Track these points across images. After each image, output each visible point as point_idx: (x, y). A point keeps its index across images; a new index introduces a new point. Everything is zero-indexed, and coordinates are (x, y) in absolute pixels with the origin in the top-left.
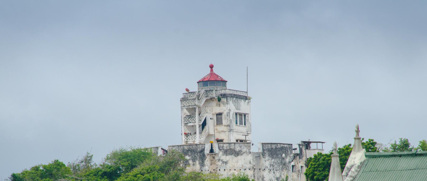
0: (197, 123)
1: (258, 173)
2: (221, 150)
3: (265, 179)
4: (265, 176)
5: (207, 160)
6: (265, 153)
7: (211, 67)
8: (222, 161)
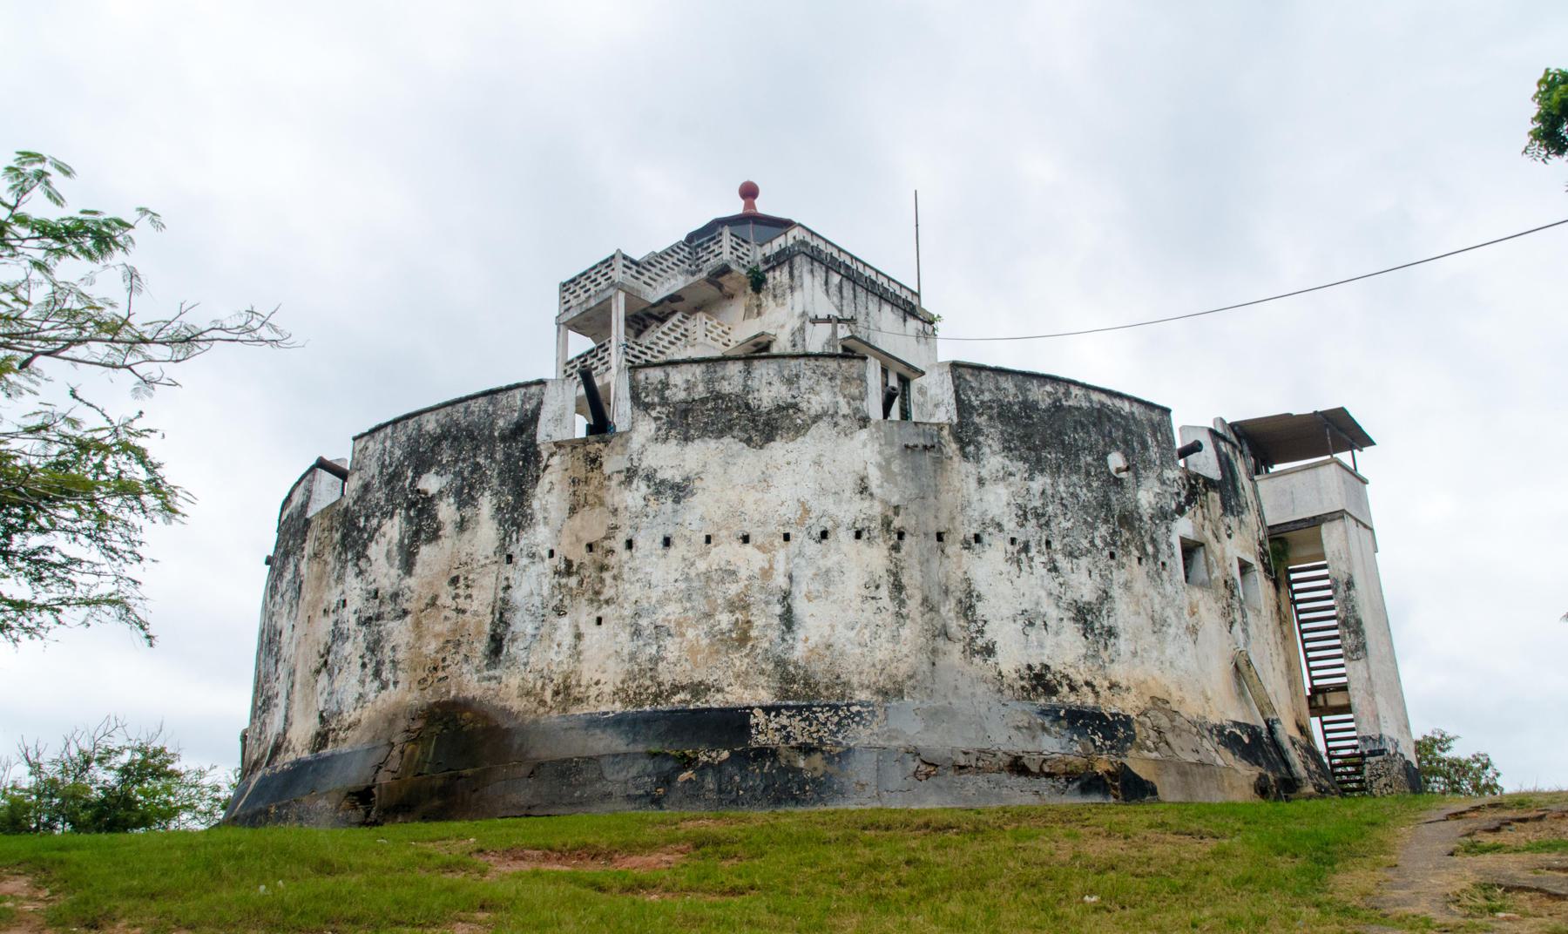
0: (614, 370)
2: (647, 407)
3: (981, 609)
4: (980, 587)
5: (546, 480)
6: (978, 431)
7: (749, 192)
8: (648, 478)
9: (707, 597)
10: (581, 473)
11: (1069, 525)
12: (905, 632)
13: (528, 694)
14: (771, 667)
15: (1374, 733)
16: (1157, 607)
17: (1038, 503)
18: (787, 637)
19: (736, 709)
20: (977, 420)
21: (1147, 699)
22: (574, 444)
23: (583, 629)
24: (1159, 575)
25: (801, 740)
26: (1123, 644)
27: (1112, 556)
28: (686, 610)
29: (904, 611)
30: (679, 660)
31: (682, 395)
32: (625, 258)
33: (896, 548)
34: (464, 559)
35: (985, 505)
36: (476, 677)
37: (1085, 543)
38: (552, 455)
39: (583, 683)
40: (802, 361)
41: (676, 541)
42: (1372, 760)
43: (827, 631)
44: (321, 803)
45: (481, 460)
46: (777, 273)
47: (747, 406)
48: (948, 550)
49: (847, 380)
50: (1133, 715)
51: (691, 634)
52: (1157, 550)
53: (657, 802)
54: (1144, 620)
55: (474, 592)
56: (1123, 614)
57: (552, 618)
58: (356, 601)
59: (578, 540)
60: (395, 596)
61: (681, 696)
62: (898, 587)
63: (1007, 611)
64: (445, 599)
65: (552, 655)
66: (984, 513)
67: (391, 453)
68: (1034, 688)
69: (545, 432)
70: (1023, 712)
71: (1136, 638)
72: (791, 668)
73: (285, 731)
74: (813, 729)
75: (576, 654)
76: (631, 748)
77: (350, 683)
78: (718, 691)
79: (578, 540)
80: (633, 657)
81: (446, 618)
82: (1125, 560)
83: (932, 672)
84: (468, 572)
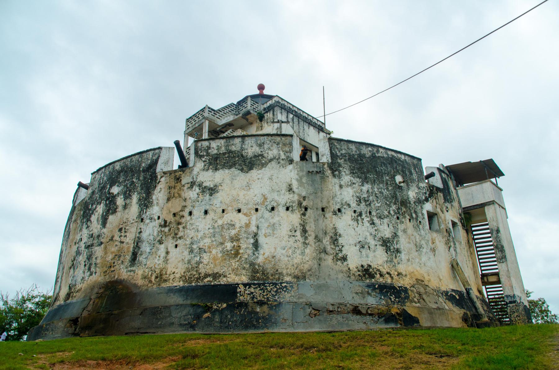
1: (316, 221)
2: (201, 157)
3: (341, 241)
6: (340, 165)
7: (261, 87)
8: (200, 186)
9: (222, 235)
10: (173, 184)
11: (379, 205)
12: (307, 251)
13: (145, 278)
14: (247, 266)
15: (512, 294)
16: (418, 240)
17: (366, 196)
18: (256, 253)
19: (231, 285)
20: (339, 161)
21: (414, 280)
22: (171, 172)
23: (169, 250)
24: (418, 226)
25: (259, 299)
26: (403, 256)
27: (398, 218)
28: (212, 241)
29: (307, 242)
30: (208, 263)
31: (215, 152)
32: (209, 108)
33: (304, 214)
34: (125, 221)
35: (343, 196)
36: (125, 270)
37: (386, 213)
38: (162, 177)
39: (168, 273)
40: (266, 137)
41: (210, 212)
42: (511, 305)
43: (273, 250)
44: (60, 324)
45: (134, 180)
46: (268, 114)
47: (242, 155)
48: (327, 215)
49: (284, 145)
50: (408, 287)
51: (214, 251)
52: (417, 216)
53: (193, 327)
54: (412, 246)
55: (128, 234)
56: (403, 243)
57: (157, 245)
58: (85, 239)
59: (170, 212)
60: (99, 236)
61: (208, 279)
62: (304, 231)
63: (352, 241)
64: (117, 238)
65: (156, 261)
66: (342, 200)
67: (103, 179)
68: (364, 275)
69: (160, 168)
70: (358, 286)
71: (409, 253)
72: (257, 267)
73: (59, 292)
74: (265, 294)
75: (166, 260)
76: (185, 302)
77: (80, 272)
78: (225, 276)
79: (170, 212)
80: (189, 262)
81: (116, 245)
82: (403, 220)
83: (319, 268)
84: (126, 226)
